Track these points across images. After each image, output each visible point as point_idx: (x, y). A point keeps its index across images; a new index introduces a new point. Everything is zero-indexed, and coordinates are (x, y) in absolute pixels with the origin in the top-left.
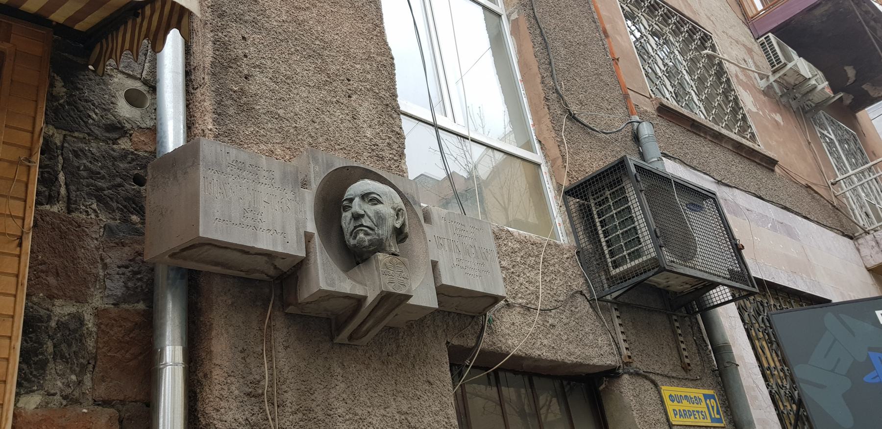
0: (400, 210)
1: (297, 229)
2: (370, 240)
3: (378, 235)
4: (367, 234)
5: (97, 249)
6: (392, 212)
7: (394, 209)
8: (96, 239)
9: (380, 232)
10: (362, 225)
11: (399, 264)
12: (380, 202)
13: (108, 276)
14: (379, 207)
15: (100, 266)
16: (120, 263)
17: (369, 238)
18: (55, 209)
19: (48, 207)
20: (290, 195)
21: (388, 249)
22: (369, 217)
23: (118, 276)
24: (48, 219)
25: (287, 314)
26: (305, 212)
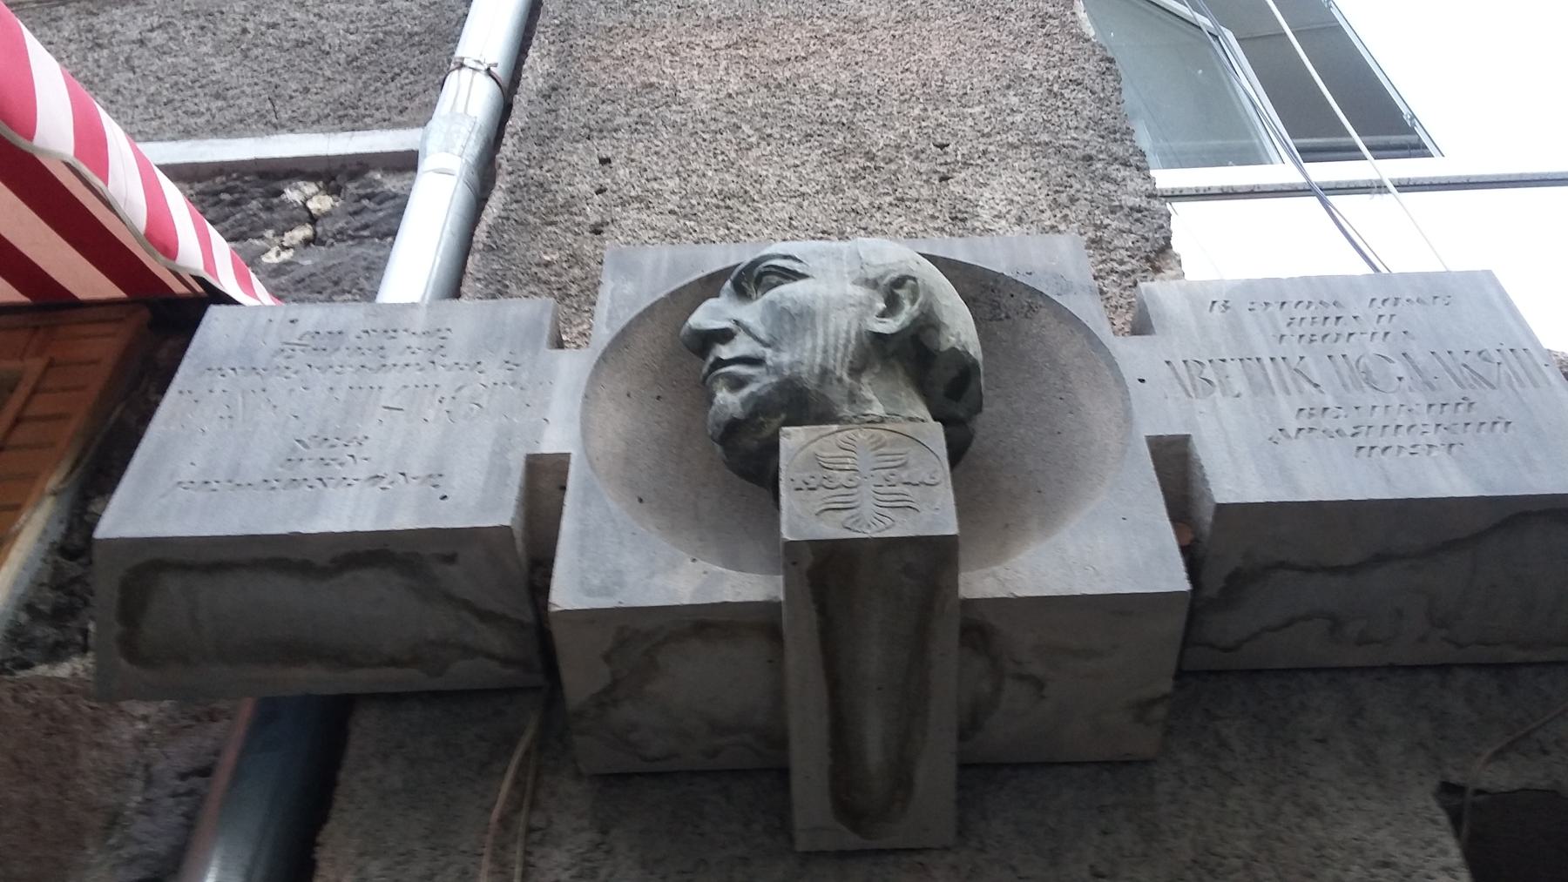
0: (900, 282)
1: (500, 452)
2: (744, 403)
3: (777, 369)
4: (737, 383)
5: (141, 742)
6: (861, 292)
7: (873, 284)
8: (145, 718)
9: (785, 358)
10: (720, 363)
11: (893, 444)
12: (794, 276)
13: (147, 809)
14: (789, 290)
15: (138, 784)
16: (184, 764)
17: (745, 392)
18: (63, 670)
19: (42, 670)
20: (494, 371)
21: (846, 411)
22: (747, 331)
23: (170, 802)
24: (30, 696)
25: (612, 781)
26: (546, 405)
